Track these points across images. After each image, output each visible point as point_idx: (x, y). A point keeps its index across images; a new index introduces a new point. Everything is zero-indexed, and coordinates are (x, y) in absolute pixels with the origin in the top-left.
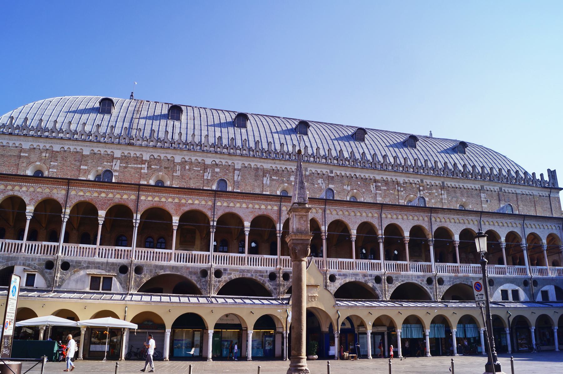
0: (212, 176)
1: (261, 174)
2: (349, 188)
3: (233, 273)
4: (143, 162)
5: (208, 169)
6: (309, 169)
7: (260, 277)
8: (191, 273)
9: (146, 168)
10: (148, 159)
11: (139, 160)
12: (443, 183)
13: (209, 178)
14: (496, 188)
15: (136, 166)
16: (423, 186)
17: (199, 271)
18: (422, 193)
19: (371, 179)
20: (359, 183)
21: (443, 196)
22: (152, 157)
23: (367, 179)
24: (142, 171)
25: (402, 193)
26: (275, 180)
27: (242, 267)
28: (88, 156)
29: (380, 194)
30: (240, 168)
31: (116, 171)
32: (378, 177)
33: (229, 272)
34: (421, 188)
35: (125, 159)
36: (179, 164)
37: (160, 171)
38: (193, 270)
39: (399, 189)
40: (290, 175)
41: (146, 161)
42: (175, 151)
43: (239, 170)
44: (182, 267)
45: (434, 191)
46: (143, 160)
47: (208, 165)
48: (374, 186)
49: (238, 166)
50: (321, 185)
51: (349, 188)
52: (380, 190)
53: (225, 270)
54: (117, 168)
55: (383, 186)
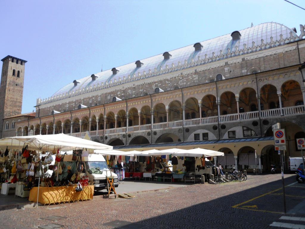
0: (92, 101)
6: (125, 87)
11: (72, 102)
12: (196, 70)
18: (181, 81)
20: (147, 86)
21: (195, 79)
25: (169, 85)
28: (61, 105)
31: (67, 108)
34: (181, 78)
35: (69, 103)
36: (83, 100)
40: (118, 92)
43: (100, 96)
50: (130, 92)
54: (67, 107)
55: (159, 84)
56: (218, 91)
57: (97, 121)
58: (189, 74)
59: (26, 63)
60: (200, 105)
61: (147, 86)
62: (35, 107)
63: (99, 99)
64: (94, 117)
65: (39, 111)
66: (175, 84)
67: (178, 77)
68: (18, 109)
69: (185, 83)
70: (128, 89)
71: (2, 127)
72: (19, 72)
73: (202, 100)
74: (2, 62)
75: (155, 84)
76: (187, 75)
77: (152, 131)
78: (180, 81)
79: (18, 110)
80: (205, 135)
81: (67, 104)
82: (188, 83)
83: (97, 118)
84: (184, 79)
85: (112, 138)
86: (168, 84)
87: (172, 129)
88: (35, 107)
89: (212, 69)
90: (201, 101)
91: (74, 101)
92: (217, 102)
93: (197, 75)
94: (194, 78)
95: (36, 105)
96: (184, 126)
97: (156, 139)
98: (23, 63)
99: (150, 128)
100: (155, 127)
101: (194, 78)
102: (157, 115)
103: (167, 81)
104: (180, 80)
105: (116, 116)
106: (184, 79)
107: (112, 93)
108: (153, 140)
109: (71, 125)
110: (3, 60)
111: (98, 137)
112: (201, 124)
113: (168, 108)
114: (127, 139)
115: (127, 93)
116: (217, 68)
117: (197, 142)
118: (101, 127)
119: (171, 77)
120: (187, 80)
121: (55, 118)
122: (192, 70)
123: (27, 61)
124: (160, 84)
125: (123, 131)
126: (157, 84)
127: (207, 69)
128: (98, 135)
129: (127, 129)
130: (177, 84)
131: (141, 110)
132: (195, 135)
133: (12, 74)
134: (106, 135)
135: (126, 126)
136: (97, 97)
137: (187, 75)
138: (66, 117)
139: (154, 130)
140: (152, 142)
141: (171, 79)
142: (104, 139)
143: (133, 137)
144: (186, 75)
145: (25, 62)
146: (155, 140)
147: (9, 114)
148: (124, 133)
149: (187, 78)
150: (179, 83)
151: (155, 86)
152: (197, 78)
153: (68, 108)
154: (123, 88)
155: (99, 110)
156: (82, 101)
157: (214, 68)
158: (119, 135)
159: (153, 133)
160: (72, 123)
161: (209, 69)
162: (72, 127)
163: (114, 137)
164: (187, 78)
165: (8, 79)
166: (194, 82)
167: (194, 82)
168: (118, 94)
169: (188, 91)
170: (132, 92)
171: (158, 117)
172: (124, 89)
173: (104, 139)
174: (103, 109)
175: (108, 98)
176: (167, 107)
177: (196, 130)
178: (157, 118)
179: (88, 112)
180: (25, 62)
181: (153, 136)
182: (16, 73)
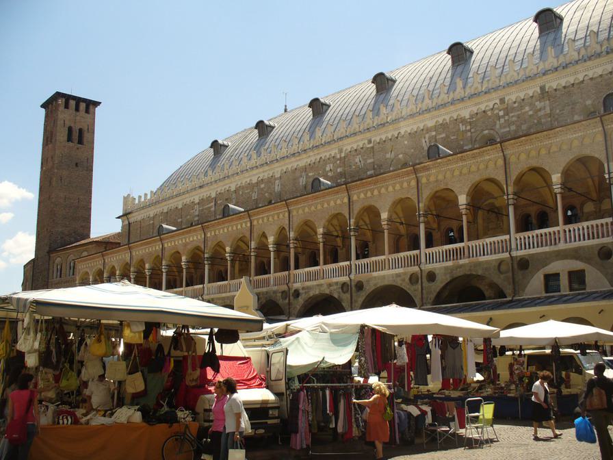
6: (344, 149)
11: (209, 199)
12: (542, 88)
18: (502, 120)
21: (541, 113)
31: (196, 216)
34: (501, 113)
40: (326, 164)
41: (213, 199)
50: (359, 163)
51: (393, 156)
54: (197, 213)
56: (609, 143)
57: (271, 247)
58: (523, 100)
59: (98, 109)
60: (559, 186)
61: (406, 142)
62: (119, 218)
63: (276, 188)
64: (264, 236)
65: (128, 229)
66: (486, 132)
67: (492, 109)
68: (82, 227)
69: (513, 128)
70: (353, 153)
71: (48, 274)
72: (81, 131)
73: (562, 174)
74: (43, 110)
75: (427, 136)
76: (520, 103)
77: (421, 270)
78: (498, 122)
79: (82, 228)
80: (577, 278)
81: (195, 205)
82: (524, 127)
83: (271, 239)
84: (511, 115)
85: (311, 294)
86: (467, 131)
87: (480, 263)
88: (119, 218)
89: (591, 79)
90: (560, 175)
91: (213, 195)
92: (607, 176)
93: (548, 101)
94: (540, 110)
95: (121, 214)
96: (514, 254)
97: (435, 294)
98: (91, 107)
99: (416, 261)
100: (430, 258)
101: (540, 110)
102: (439, 224)
103: (461, 125)
104: (499, 118)
105: (320, 231)
106: (511, 115)
107: (311, 167)
108: (425, 296)
109: (206, 262)
110: (43, 106)
111: (275, 292)
112: (562, 246)
113: (465, 202)
114: (354, 294)
115: (350, 166)
116: (606, 77)
117: (553, 297)
118: (284, 266)
119: (472, 113)
120: (518, 117)
121: (166, 245)
122: (532, 89)
123: (100, 103)
124: (443, 132)
125: (342, 272)
126: (434, 133)
127: (577, 82)
128: (275, 288)
129: (353, 267)
130: (492, 132)
131: (389, 211)
132: (548, 277)
133: (66, 138)
134: (297, 285)
135: (349, 259)
136: (270, 181)
137: (520, 103)
138: (191, 239)
139: (428, 267)
140: (424, 301)
141: (472, 117)
142: (292, 298)
143: (369, 288)
144: (515, 103)
145: (97, 104)
146: (433, 296)
147: (62, 238)
148: (345, 279)
149: (520, 112)
150: (498, 126)
151: (427, 141)
152: (548, 110)
153: (198, 216)
154: (341, 151)
155: (276, 217)
156: (234, 196)
157: (596, 78)
158: (330, 285)
159: (425, 275)
160: (206, 256)
161: (582, 82)
162: (207, 267)
163: (317, 293)
164: (520, 112)
165: (57, 152)
166: (539, 123)
167: (539, 123)
168: (328, 169)
169: (521, 148)
170: (365, 160)
171: (442, 228)
172: (343, 155)
173: (292, 298)
174: (287, 214)
175: (301, 184)
176: (463, 200)
177: (550, 263)
178: (439, 233)
179: (246, 223)
180: (97, 104)
181: (424, 285)
182: (75, 135)
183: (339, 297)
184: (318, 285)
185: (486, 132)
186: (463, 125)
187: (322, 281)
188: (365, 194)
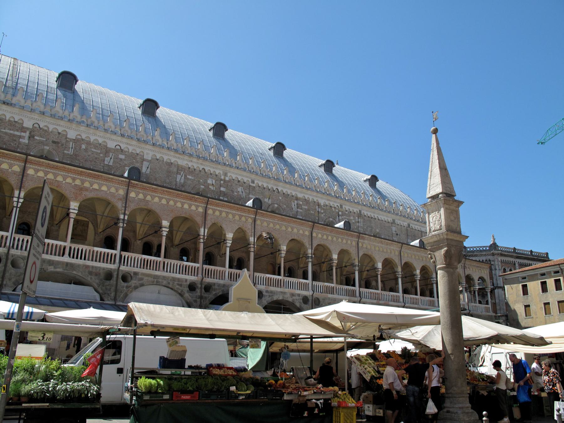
1: (175, 170)
2: (270, 202)
3: (146, 278)
4: (23, 129)
5: (111, 154)
6: (229, 174)
7: (178, 286)
8: (90, 273)
9: (27, 138)
10: (31, 127)
12: (360, 211)
13: (111, 164)
14: (405, 224)
15: (12, 132)
16: (342, 212)
17: (101, 271)
19: (293, 196)
20: (280, 198)
21: (360, 224)
22: (36, 126)
23: (288, 195)
24: (21, 140)
25: (322, 215)
26: (190, 179)
27: (157, 273)
29: (301, 212)
30: (150, 159)
32: (300, 195)
33: (140, 276)
34: (340, 213)
37: (47, 145)
38: (94, 271)
39: (320, 210)
40: (208, 177)
41: (28, 129)
42: (68, 124)
43: (148, 161)
44: (79, 266)
45: (352, 218)
46: (23, 127)
47: (110, 149)
48: (295, 204)
49: (148, 157)
50: (241, 193)
52: (301, 209)
53: (136, 274)
66: (331, 219)
85: (275, 298)
121: (30, 172)
126: (301, 203)
138: (96, 186)
158: (293, 295)
163: (281, 298)
183: (301, 306)
184: (281, 292)
185: (331, 219)
186: (319, 208)
187: (287, 290)
188: (323, 236)
